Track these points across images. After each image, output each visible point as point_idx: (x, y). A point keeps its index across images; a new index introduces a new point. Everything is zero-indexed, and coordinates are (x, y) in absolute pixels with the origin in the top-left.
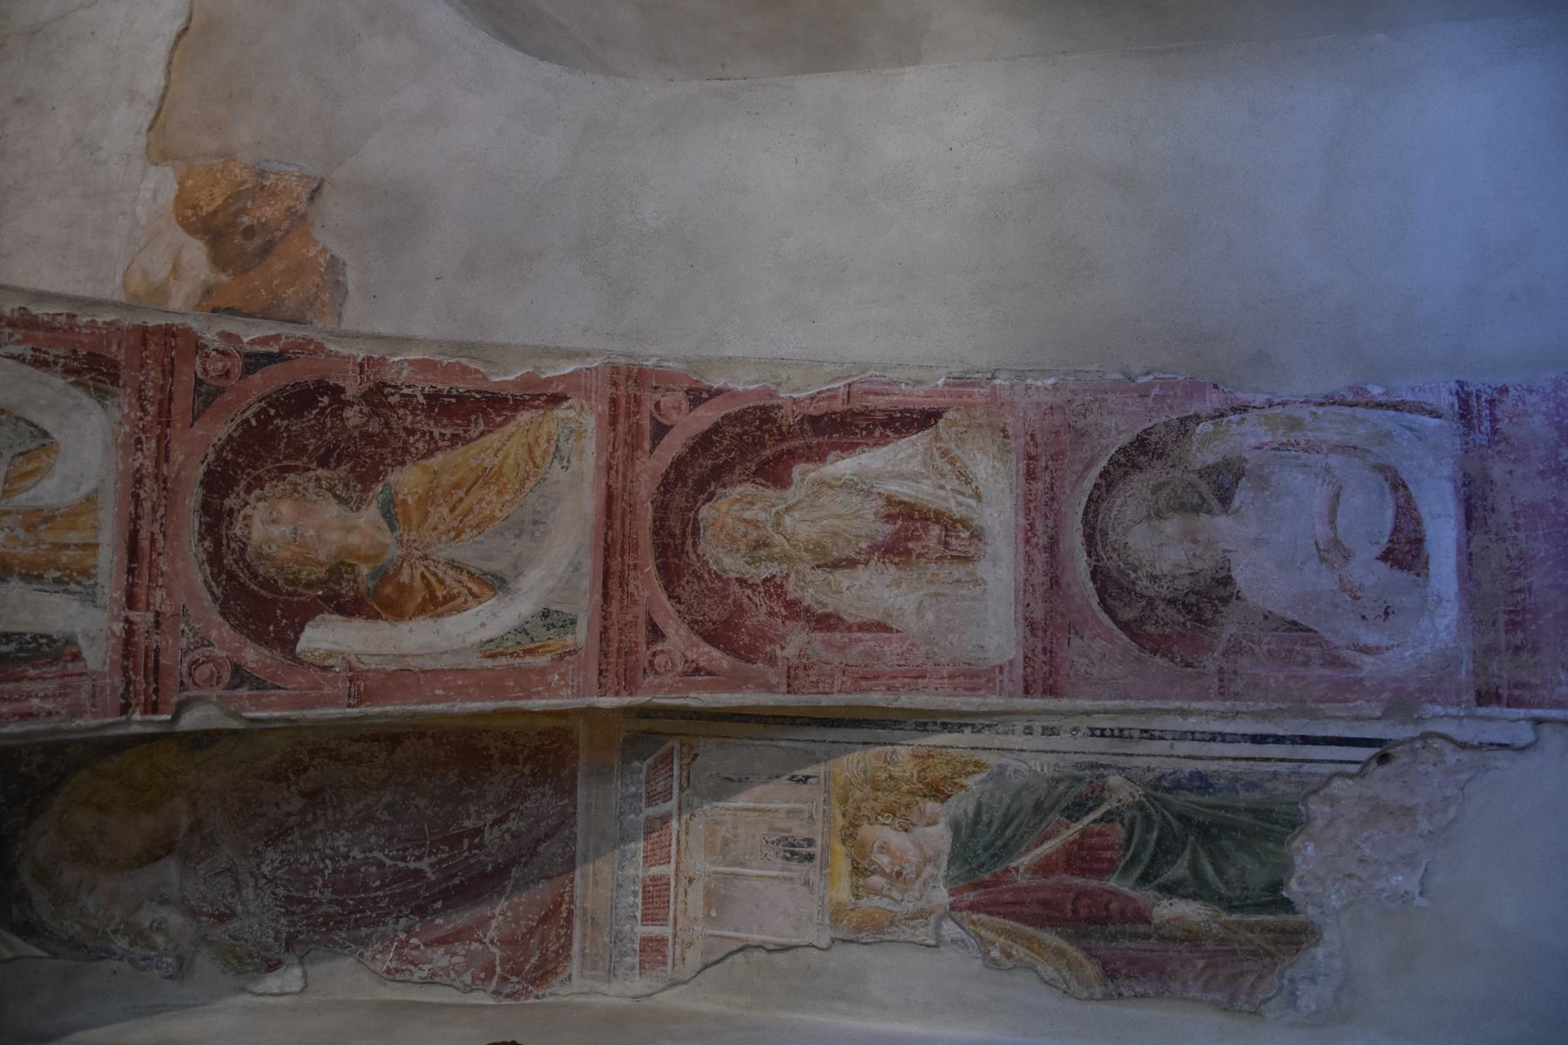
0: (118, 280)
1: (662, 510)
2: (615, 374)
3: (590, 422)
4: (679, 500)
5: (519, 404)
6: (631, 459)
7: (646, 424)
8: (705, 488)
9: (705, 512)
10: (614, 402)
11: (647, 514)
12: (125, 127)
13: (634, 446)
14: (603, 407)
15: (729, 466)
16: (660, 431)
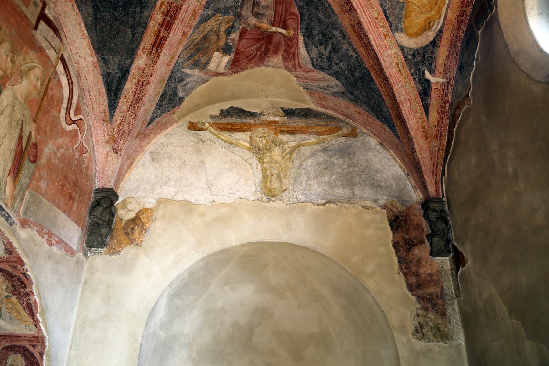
0: (131, 196)
1: (19, 347)
2: (43, 337)
3: (33, 332)
4: (21, 350)
5: (34, 319)
6: (28, 340)
7: (34, 344)
8: (24, 355)
9: (19, 355)
10: (38, 337)
11: (18, 344)
12: (168, 191)
13: (30, 341)
14: (36, 335)
15: (28, 360)
16: (34, 346)
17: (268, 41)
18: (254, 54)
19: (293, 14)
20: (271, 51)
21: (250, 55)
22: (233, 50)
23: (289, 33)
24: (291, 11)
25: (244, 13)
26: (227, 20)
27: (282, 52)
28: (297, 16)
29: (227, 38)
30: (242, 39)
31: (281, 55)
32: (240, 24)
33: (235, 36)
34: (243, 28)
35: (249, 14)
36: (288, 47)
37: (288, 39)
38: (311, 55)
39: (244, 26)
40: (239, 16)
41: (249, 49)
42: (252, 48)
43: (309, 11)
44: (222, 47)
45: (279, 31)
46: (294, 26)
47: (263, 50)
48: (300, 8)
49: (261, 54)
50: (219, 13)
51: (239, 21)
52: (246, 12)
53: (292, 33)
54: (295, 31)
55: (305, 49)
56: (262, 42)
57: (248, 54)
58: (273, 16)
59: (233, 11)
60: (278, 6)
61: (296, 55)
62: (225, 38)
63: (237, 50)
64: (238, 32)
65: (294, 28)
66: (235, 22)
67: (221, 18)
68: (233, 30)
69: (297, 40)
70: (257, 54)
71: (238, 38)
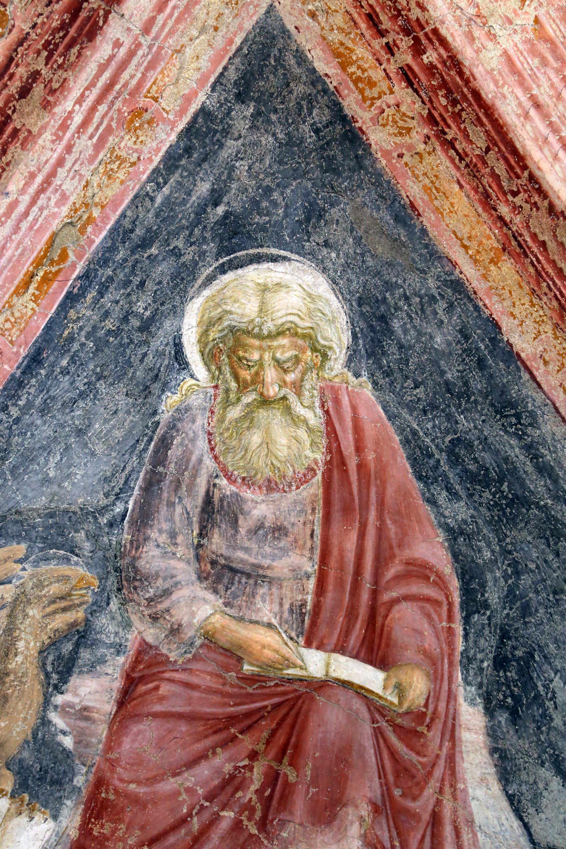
17: (280, 738)
18: (196, 824)
19: (420, 571)
20: (300, 805)
21: (174, 828)
22: (79, 781)
23: (400, 690)
24: (407, 553)
25: (151, 558)
26: (55, 589)
27: (365, 810)
28: (441, 583)
29: (47, 702)
30: (136, 717)
31: (355, 830)
32: (127, 625)
33: (94, 690)
34: (144, 648)
35: (183, 569)
36: (402, 776)
37: (397, 728)
38: (536, 828)
39: (152, 634)
40: (123, 577)
41: (170, 785)
42: (189, 779)
43: (506, 552)
44: (12, 749)
45: (344, 675)
46: (430, 641)
47: (249, 794)
48: (454, 534)
49: (237, 825)
50: (18, 538)
51: (124, 603)
52: (166, 555)
53: (418, 686)
54: (435, 677)
55: (496, 788)
56: (247, 743)
57: (161, 817)
58: (311, 584)
59: (94, 538)
60: (336, 526)
61: (448, 830)
62: (38, 698)
63: (100, 783)
64: (115, 668)
65: (426, 653)
66: (97, 608)
67: (25, 573)
68: (85, 655)
69: (451, 733)
70: (216, 819)
71: (109, 707)
